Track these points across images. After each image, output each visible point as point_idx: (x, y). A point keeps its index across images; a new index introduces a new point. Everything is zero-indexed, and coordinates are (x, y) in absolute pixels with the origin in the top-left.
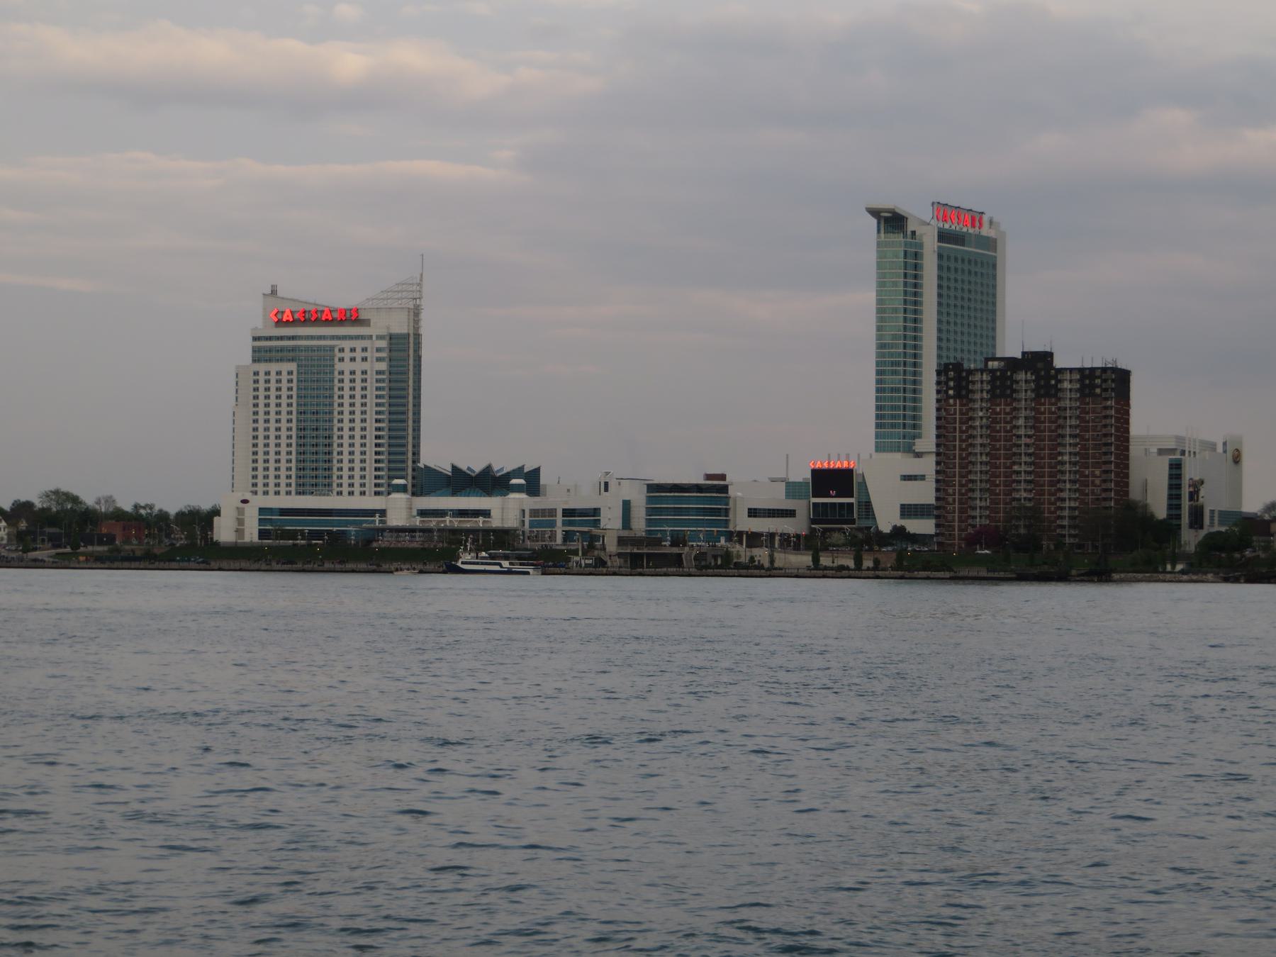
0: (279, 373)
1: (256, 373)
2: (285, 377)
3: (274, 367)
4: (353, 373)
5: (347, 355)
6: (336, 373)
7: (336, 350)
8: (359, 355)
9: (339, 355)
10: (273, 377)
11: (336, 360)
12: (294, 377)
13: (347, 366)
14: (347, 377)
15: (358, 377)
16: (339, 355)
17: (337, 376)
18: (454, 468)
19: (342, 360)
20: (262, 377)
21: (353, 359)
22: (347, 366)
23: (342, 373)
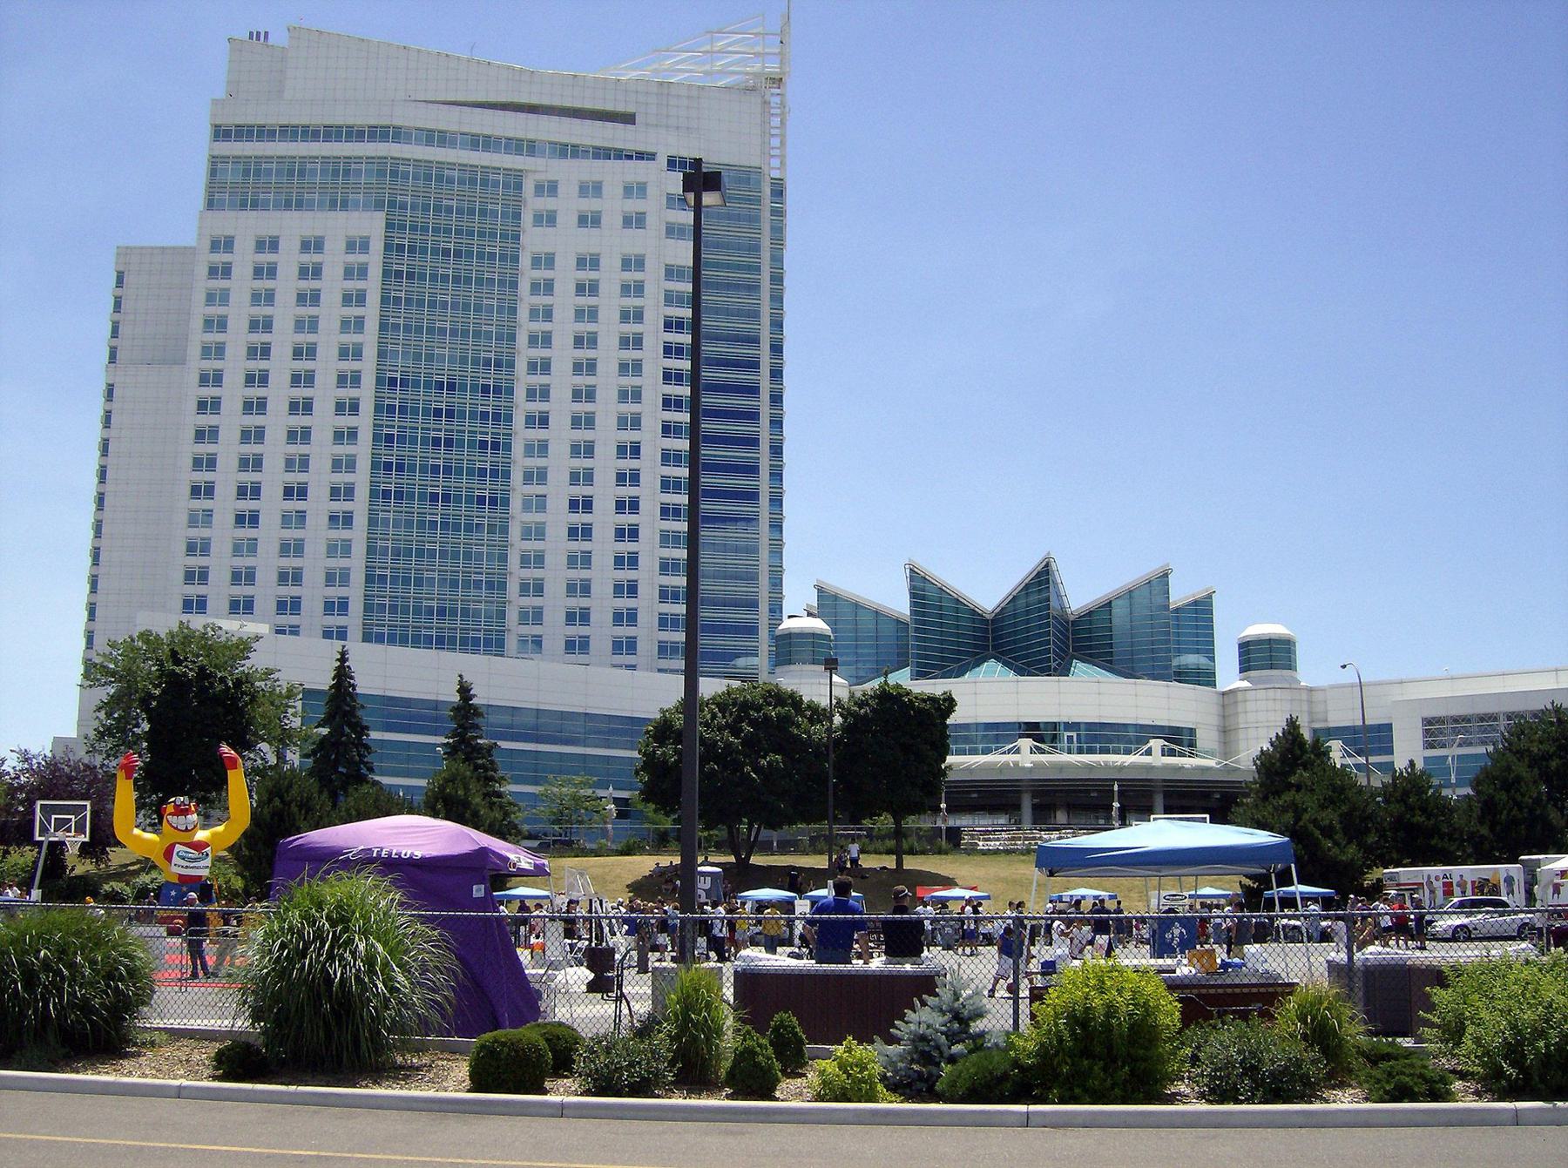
0: (312, 245)
1: (223, 244)
2: (334, 259)
3: (292, 226)
4: (588, 262)
5: (568, 205)
6: (525, 261)
7: (528, 187)
8: (613, 205)
9: (546, 203)
10: (289, 259)
11: (527, 218)
12: (375, 259)
13: (566, 241)
14: (566, 276)
15: (610, 277)
16: (546, 203)
17: (528, 274)
18: (922, 589)
19: (548, 219)
20: (244, 259)
21: (589, 220)
22: (566, 241)
23: (549, 261)
